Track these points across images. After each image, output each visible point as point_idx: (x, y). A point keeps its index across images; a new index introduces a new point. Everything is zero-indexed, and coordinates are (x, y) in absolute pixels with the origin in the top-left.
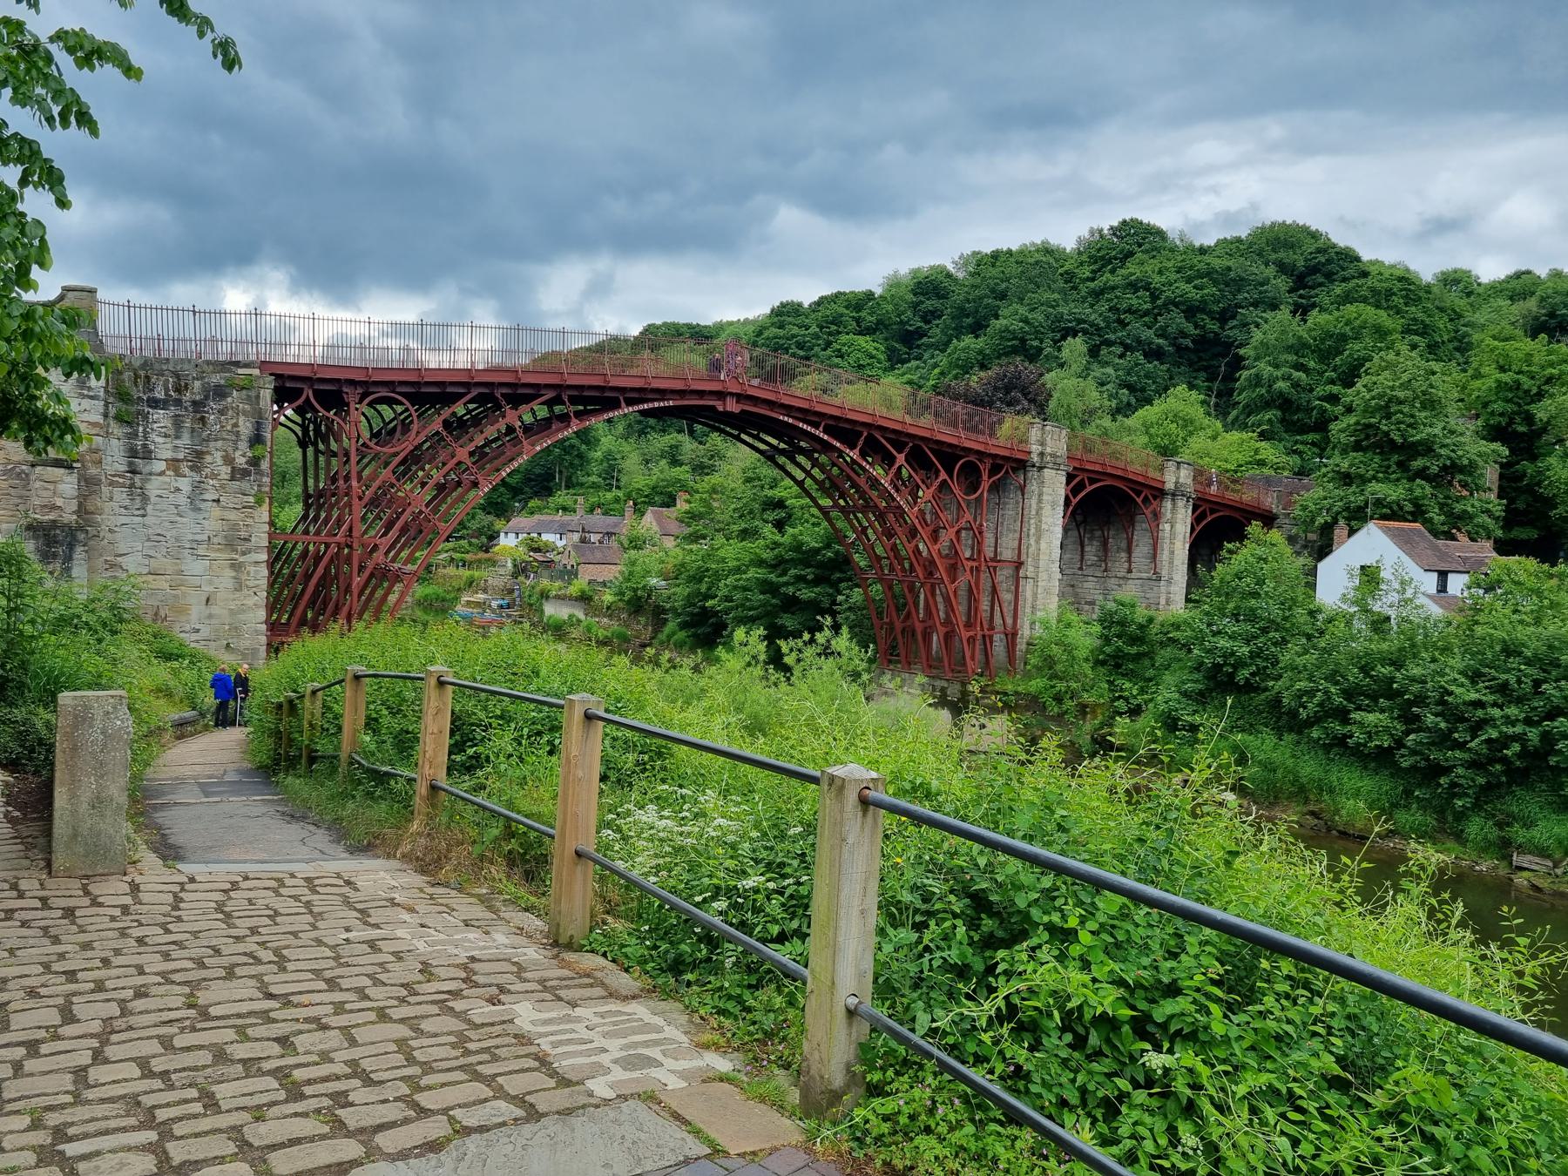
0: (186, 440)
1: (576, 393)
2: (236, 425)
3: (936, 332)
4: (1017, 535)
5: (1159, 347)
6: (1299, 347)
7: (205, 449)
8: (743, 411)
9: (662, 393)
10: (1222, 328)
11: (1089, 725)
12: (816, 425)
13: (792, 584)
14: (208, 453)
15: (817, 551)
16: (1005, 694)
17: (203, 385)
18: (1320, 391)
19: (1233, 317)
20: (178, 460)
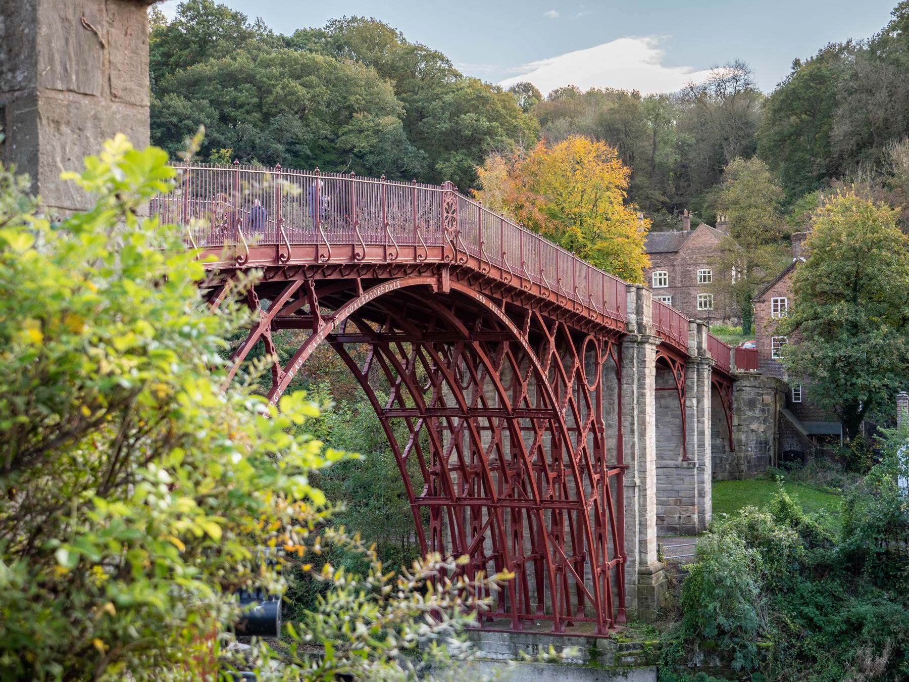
1: (318, 277)
4: (614, 431)
8: (452, 290)
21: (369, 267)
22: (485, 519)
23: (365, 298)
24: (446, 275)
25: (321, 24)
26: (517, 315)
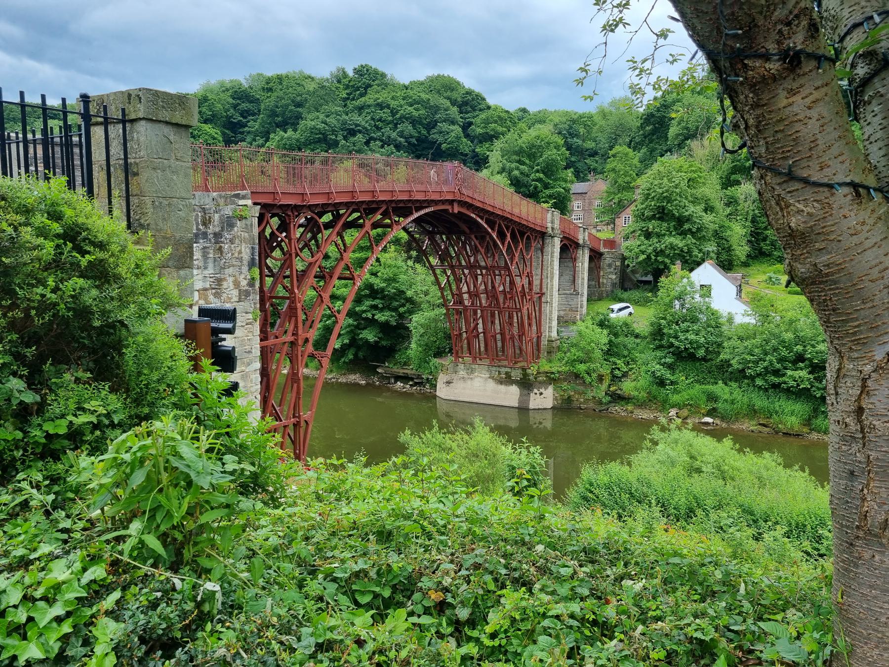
0: (210, 270)
1: (394, 205)
2: (240, 252)
3: (254, 125)
4: (539, 277)
5: (400, 142)
6: (520, 152)
7: (222, 276)
9: (430, 203)
10: (428, 133)
11: (604, 386)
12: (482, 219)
13: (369, 311)
14: (225, 279)
15: (383, 290)
16: (553, 373)
17: (220, 217)
18: (533, 176)
19: (433, 128)
20: (205, 290)
21: (417, 201)
22: (479, 315)
23: (416, 215)
24: (456, 205)
25: (422, 78)
26: (491, 224)
